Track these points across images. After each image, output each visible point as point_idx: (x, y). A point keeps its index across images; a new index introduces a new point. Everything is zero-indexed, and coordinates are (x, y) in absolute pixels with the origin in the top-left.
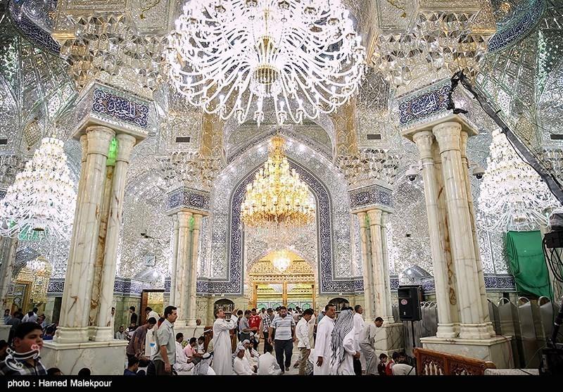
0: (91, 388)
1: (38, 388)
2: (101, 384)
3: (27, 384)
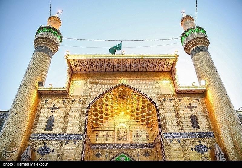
0: (39, 166)
1: (16, 166)
2: (44, 164)
3: (12, 164)
